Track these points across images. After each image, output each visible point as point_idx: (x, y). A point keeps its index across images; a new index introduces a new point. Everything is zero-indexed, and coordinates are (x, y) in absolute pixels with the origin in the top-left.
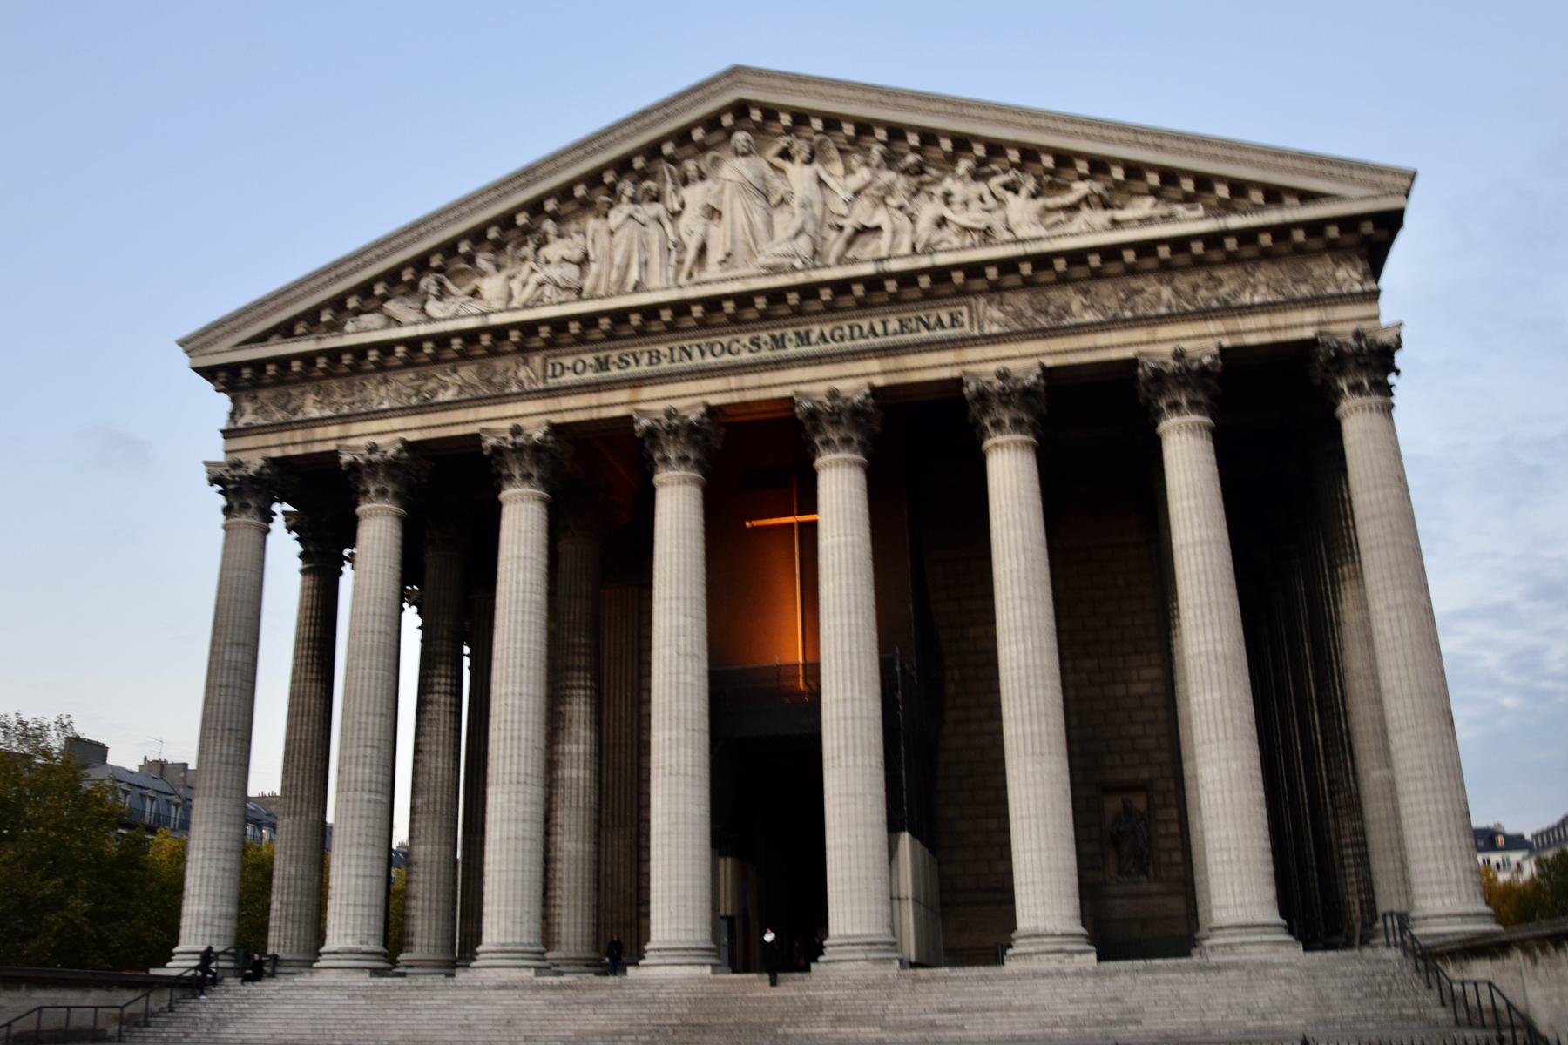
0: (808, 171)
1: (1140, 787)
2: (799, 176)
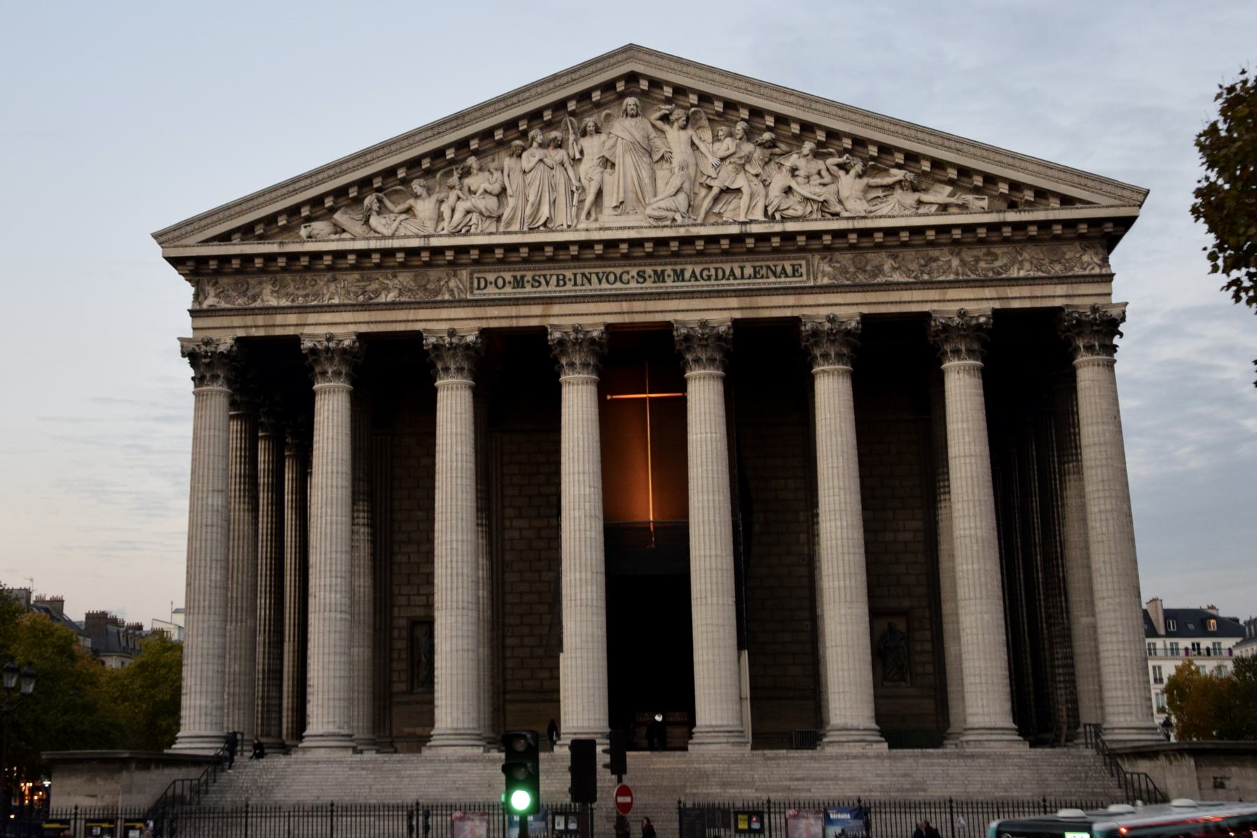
0: (685, 135)
1: (905, 613)
2: (676, 139)
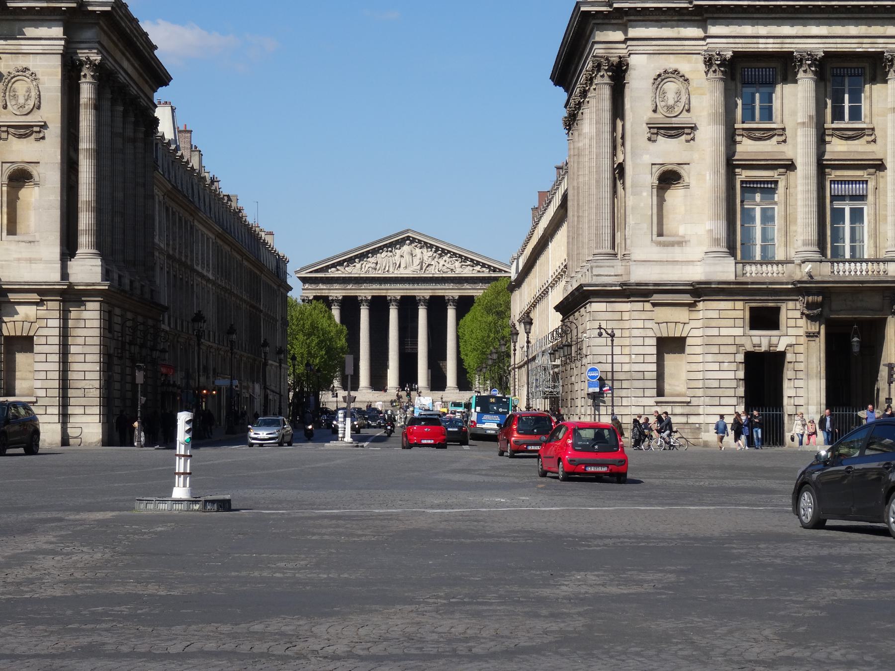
2: (418, 251)
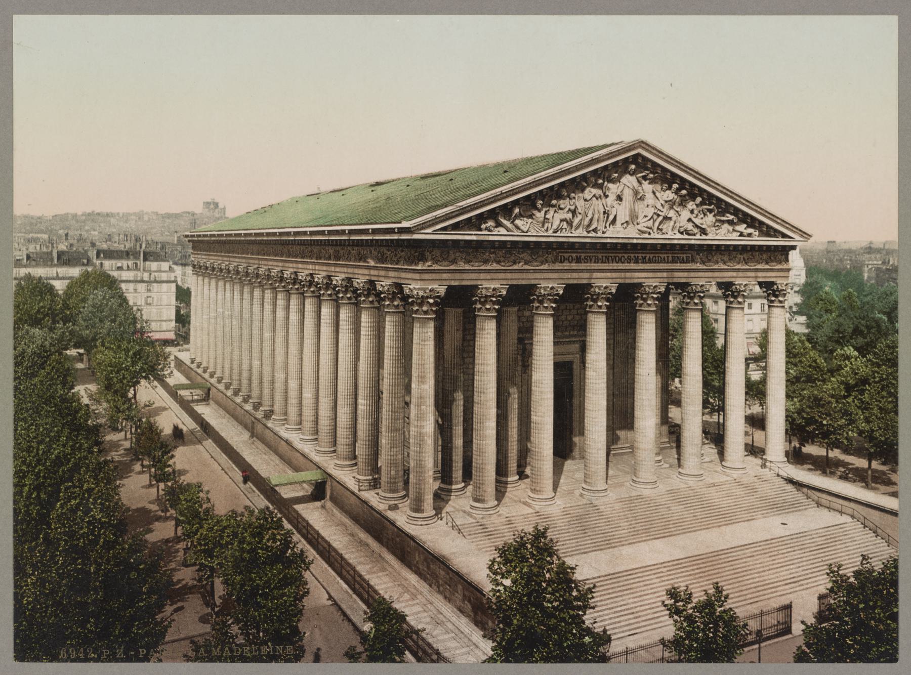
0: (651, 186)
2: (647, 187)
